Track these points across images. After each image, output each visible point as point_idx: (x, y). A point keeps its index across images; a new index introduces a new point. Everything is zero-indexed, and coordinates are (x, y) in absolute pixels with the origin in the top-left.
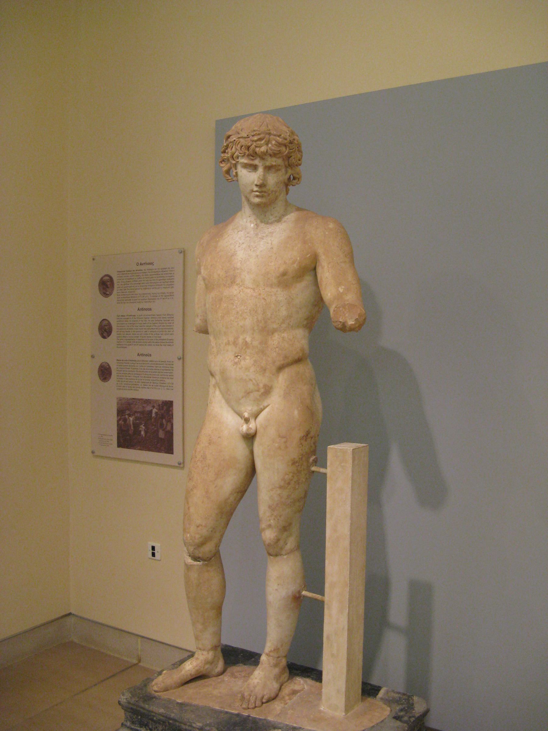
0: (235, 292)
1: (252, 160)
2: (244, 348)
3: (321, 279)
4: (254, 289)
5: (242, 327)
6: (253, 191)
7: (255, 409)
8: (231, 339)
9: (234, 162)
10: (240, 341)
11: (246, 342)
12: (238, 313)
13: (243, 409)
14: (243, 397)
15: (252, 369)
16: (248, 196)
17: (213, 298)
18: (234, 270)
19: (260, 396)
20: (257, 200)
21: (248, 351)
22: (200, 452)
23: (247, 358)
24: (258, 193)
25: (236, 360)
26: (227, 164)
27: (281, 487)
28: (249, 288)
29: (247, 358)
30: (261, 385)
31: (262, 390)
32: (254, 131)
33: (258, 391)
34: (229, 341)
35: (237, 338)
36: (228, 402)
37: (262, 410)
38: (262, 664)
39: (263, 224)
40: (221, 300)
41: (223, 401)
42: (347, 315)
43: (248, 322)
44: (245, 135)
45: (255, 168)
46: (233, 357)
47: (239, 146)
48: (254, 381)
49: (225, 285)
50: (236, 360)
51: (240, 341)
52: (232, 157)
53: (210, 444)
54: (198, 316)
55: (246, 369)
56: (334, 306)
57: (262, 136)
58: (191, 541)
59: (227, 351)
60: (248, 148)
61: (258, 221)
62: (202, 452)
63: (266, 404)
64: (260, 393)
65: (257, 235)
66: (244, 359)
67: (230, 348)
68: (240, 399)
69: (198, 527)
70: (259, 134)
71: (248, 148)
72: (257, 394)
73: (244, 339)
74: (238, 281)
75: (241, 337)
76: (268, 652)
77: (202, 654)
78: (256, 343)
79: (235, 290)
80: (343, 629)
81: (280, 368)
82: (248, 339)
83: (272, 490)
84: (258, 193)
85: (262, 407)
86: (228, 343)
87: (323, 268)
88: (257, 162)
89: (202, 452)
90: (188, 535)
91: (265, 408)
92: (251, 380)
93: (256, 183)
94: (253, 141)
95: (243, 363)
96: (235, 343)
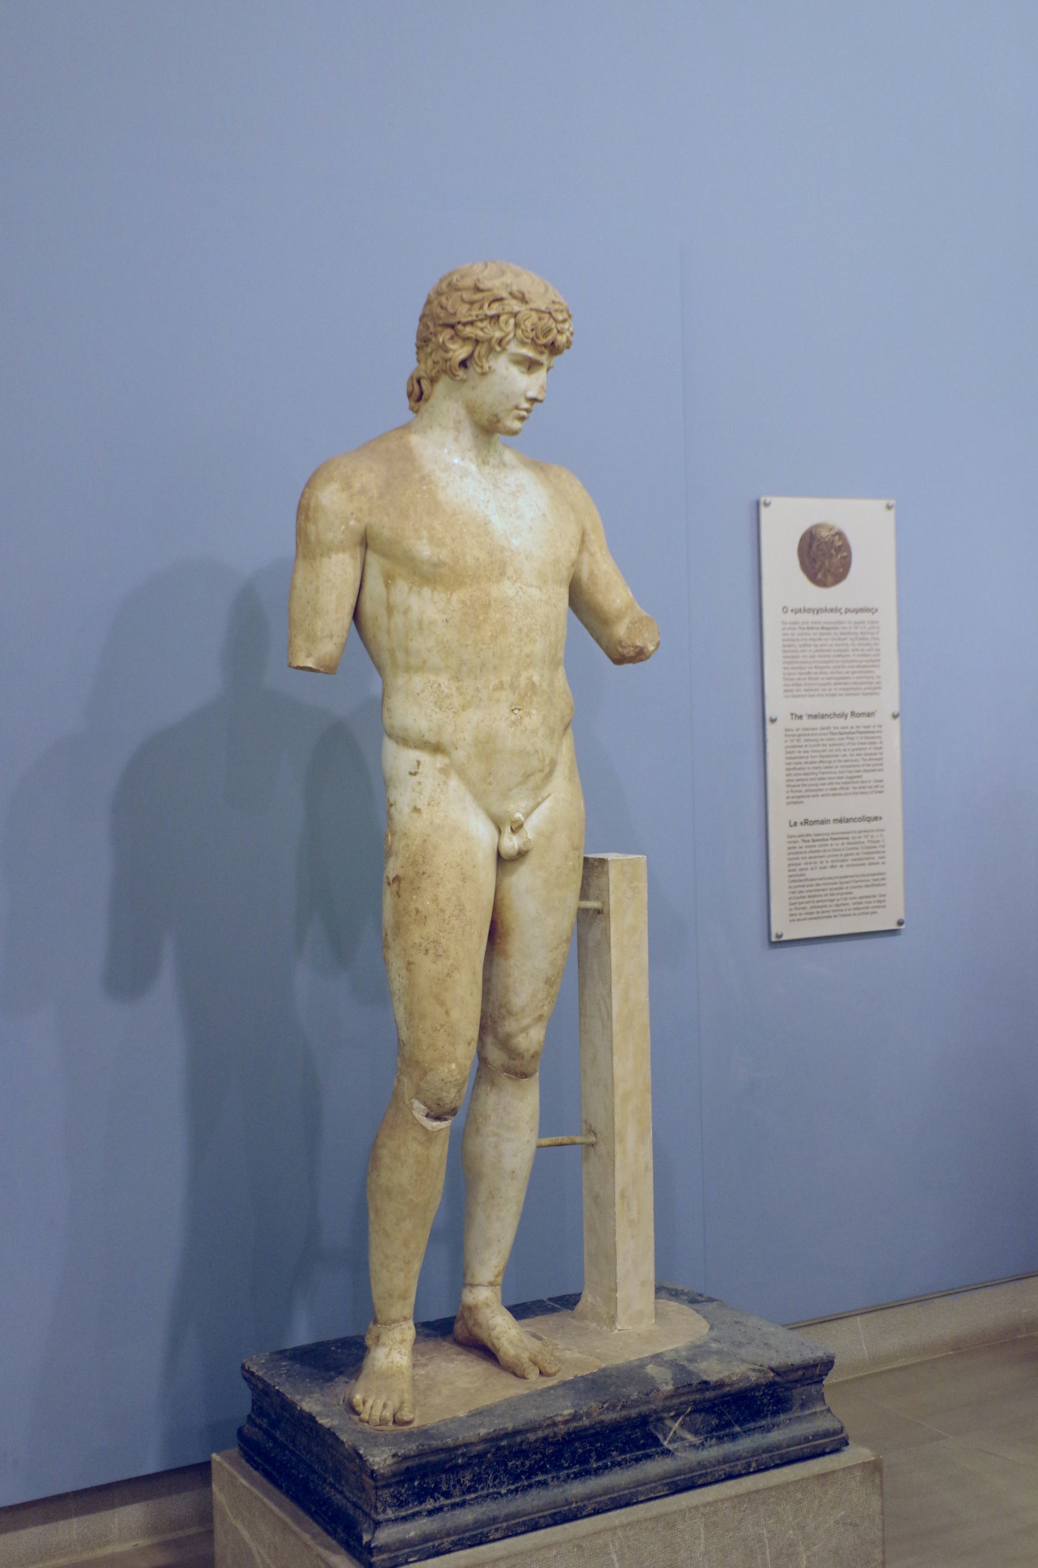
0: (511, 592)
1: (542, 353)
2: (529, 693)
3: (592, 574)
4: (540, 588)
5: (528, 656)
6: (517, 408)
7: (531, 803)
8: (506, 678)
9: (498, 349)
10: (523, 681)
11: (533, 683)
12: (520, 630)
13: (512, 807)
14: (517, 785)
15: (541, 732)
16: (501, 415)
17: (463, 602)
18: (501, 552)
19: (543, 780)
20: (517, 425)
21: (535, 699)
22: (448, 899)
23: (534, 712)
24: (524, 413)
25: (513, 717)
26: (462, 347)
27: (568, 940)
28: (531, 586)
29: (534, 712)
30: (547, 761)
31: (547, 770)
32: (554, 302)
33: (542, 771)
34: (502, 683)
35: (518, 675)
36: (479, 797)
37: (539, 804)
38: (487, 1305)
39: (487, 467)
40: (487, 606)
41: (469, 797)
42: (646, 635)
43: (539, 647)
44: (543, 308)
45: (531, 365)
46: (507, 711)
47: (528, 324)
48: (541, 755)
49: (489, 579)
50: (513, 717)
51: (523, 681)
52: (500, 342)
53: (464, 880)
54: (332, 637)
55: (533, 732)
56: (627, 620)
57: (565, 316)
58: (458, 1077)
59: (498, 701)
60: (547, 332)
61: (480, 460)
62: (454, 898)
63: (545, 794)
64: (542, 775)
65: (495, 486)
66: (529, 714)
67: (503, 695)
68: (510, 790)
69: (469, 1044)
70: (562, 311)
71: (547, 332)
72: (538, 777)
73: (530, 678)
74: (510, 571)
75: (525, 674)
76: (491, 1278)
77: (409, 1328)
78: (545, 685)
79: (507, 589)
80: (646, 1167)
81: (566, 729)
82: (536, 678)
83: (556, 948)
84: (524, 413)
85: (540, 799)
86: (501, 686)
87: (592, 555)
88: (544, 358)
89: (454, 898)
90: (453, 1066)
91: (544, 799)
92: (536, 751)
93: (531, 394)
94: (556, 321)
95: (526, 720)
96: (513, 687)
